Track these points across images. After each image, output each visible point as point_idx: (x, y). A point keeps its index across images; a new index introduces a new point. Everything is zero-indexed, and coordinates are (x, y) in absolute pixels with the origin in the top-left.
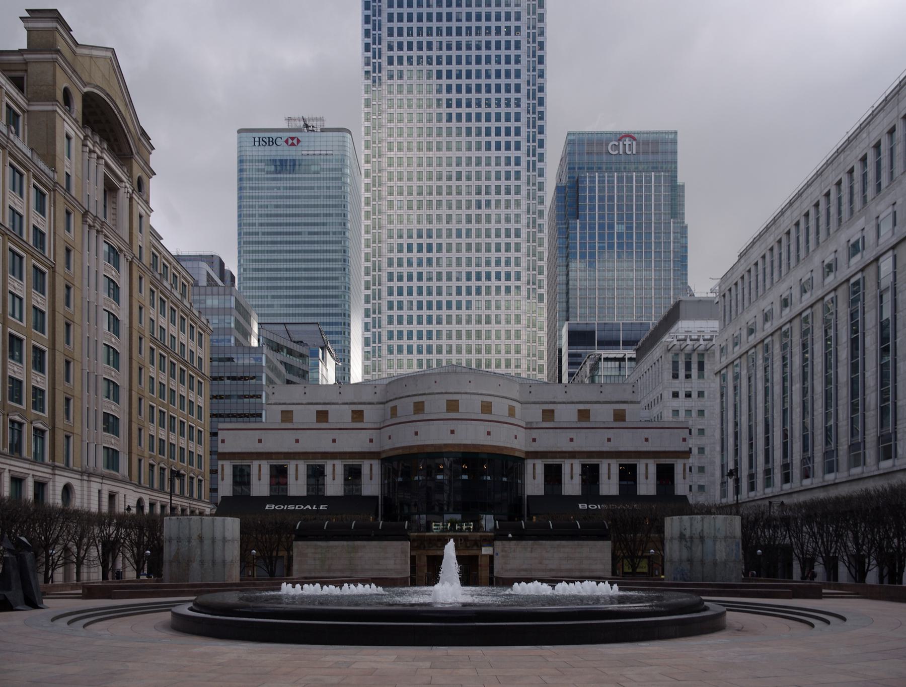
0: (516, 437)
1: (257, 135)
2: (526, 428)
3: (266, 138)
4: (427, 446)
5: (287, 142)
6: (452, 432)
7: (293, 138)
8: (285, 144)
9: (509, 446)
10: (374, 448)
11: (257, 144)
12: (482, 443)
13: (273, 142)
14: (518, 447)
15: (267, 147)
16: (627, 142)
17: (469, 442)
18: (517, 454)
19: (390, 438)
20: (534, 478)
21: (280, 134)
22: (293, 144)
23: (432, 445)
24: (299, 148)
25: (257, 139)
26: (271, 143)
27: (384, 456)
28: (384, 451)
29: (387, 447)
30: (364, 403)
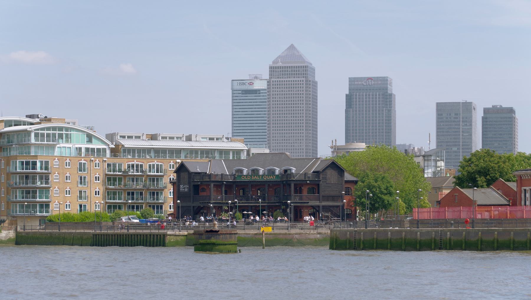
1: (238, 82)
3: (242, 82)
5: (249, 84)
7: (251, 83)
8: (248, 85)
11: (238, 85)
13: (244, 84)
15: (242, 86)
16: (370, 81)
21: (246, 81)
22: (251, 85)
24: (253, 86)
25: (238, 83)
26: (243, 84)
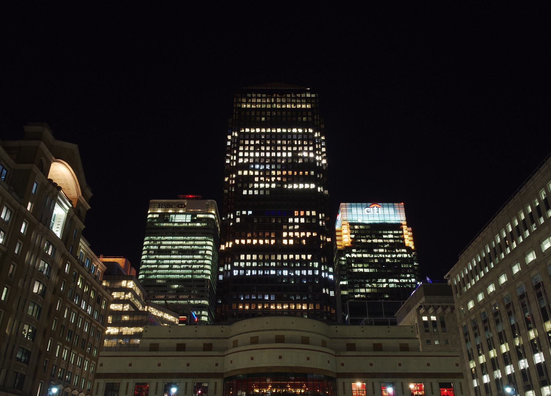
0: (329, 362)
2: (336, 356)
4: (261, 368)
6: (280, 357)
9: (324, 368)
10: (218, 370)
12: (303, 366)
14: (331, 369)
17: (293, 365)
18: (330, 375)
19: (231, 362)
20: (344, 393)
23: (264, 367)
27: (226, 376)
28: (227, 373)
29: (229, 369)
30: (213, 338)
